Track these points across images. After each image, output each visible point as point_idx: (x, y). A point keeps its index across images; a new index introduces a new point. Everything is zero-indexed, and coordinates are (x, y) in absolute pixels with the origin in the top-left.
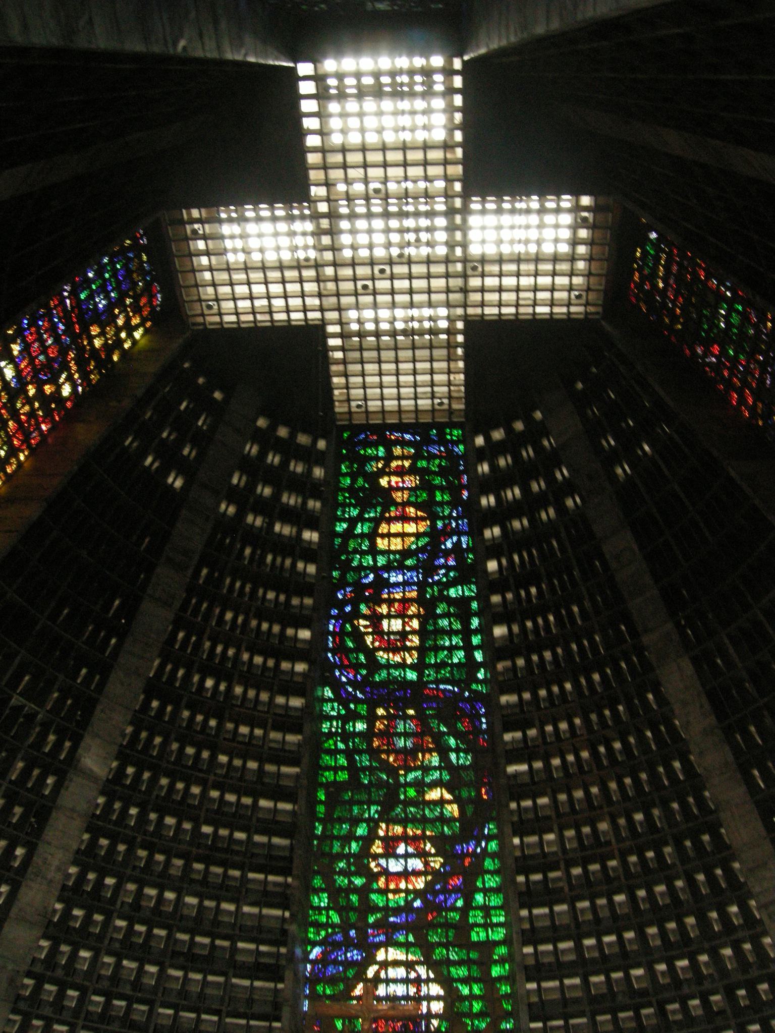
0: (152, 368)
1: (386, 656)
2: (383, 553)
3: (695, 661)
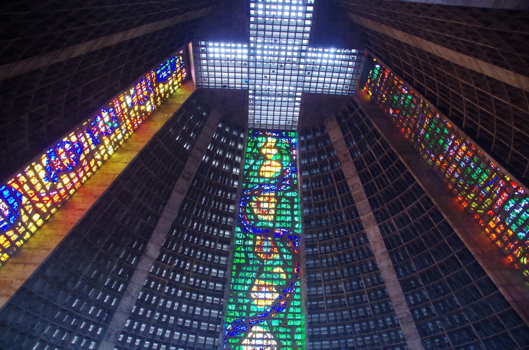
0: (181, 101)
1: (261, 217)
3: (380, 227)
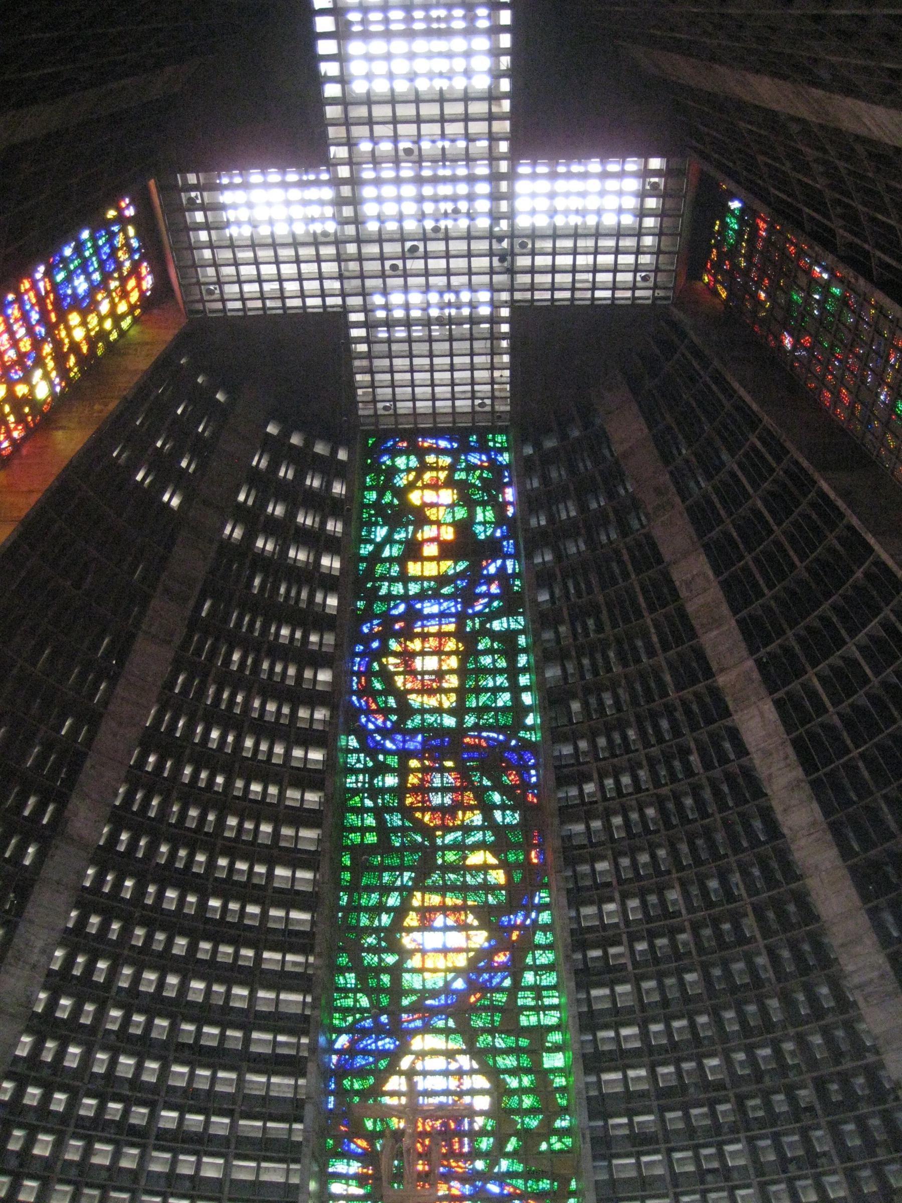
0: (142, 363)
1: (419, 699)
2: (415, 579)
3: (779, 704)
